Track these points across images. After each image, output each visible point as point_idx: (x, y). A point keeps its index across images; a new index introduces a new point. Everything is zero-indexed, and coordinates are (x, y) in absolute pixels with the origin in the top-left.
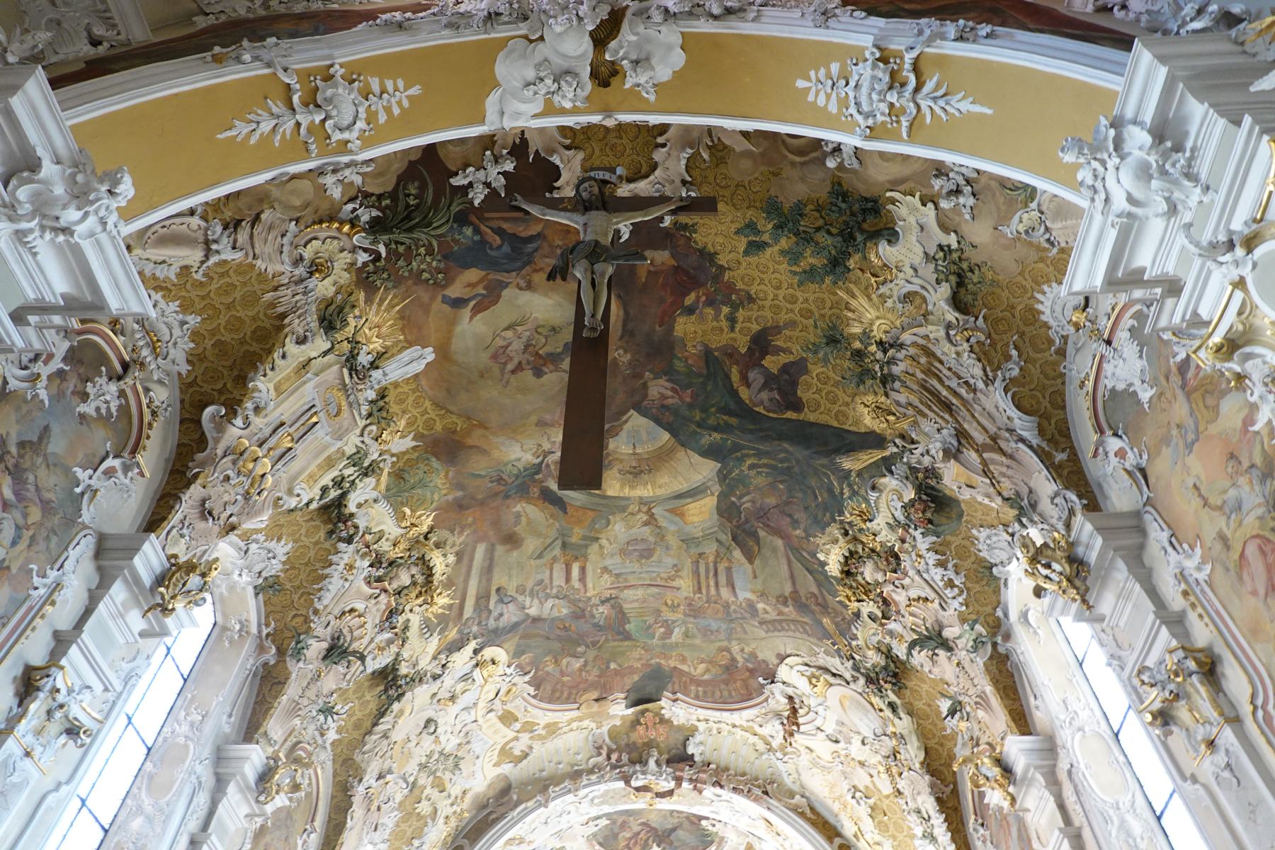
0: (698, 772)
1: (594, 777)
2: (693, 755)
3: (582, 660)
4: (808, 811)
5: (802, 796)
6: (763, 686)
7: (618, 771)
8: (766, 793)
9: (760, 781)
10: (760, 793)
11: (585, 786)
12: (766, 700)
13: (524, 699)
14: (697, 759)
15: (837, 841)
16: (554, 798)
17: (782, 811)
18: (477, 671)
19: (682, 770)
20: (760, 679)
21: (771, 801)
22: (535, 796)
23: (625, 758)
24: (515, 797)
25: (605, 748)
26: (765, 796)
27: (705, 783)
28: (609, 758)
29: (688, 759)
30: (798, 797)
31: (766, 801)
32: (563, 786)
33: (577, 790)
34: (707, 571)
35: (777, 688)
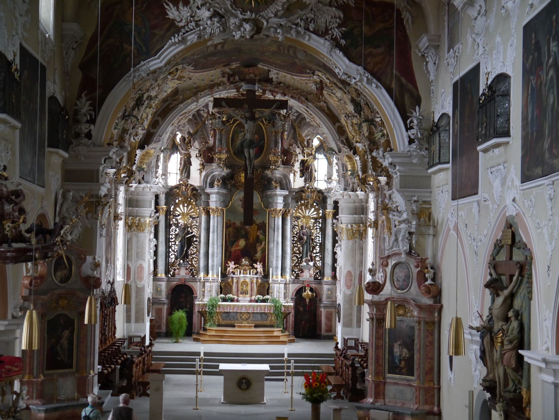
0: (275, 88)
1: (221, 88)
2: (272, 78)
3: (218, 57)
4: (326, 109)
5: (325, 102)
6: (309, 73)
7: (233, 85)
8: (307, 99)
9: (305, 93)
10: (304, 99)
11: (216, 92)
12: (310, 77)
13: (189, 72)
14: (274, 80)
15: (337, 124)
16: (201, 98)
17: (314, 109)
18: (169, 77)
19: (266, 87)
20: (308, 71)
21: (309, 103)
22: (191, 97)
23: (237, 78)
24: (181, 97)
25: (227, 76)
26: (306, 101)
27: (277, 93)
28: (229, 79)
29: (270, 81)
30: (322, 103)
31: (306, 103)
32: (205, 92)
33: (213, 94)
34: (284, 49)
35: (315, 77)
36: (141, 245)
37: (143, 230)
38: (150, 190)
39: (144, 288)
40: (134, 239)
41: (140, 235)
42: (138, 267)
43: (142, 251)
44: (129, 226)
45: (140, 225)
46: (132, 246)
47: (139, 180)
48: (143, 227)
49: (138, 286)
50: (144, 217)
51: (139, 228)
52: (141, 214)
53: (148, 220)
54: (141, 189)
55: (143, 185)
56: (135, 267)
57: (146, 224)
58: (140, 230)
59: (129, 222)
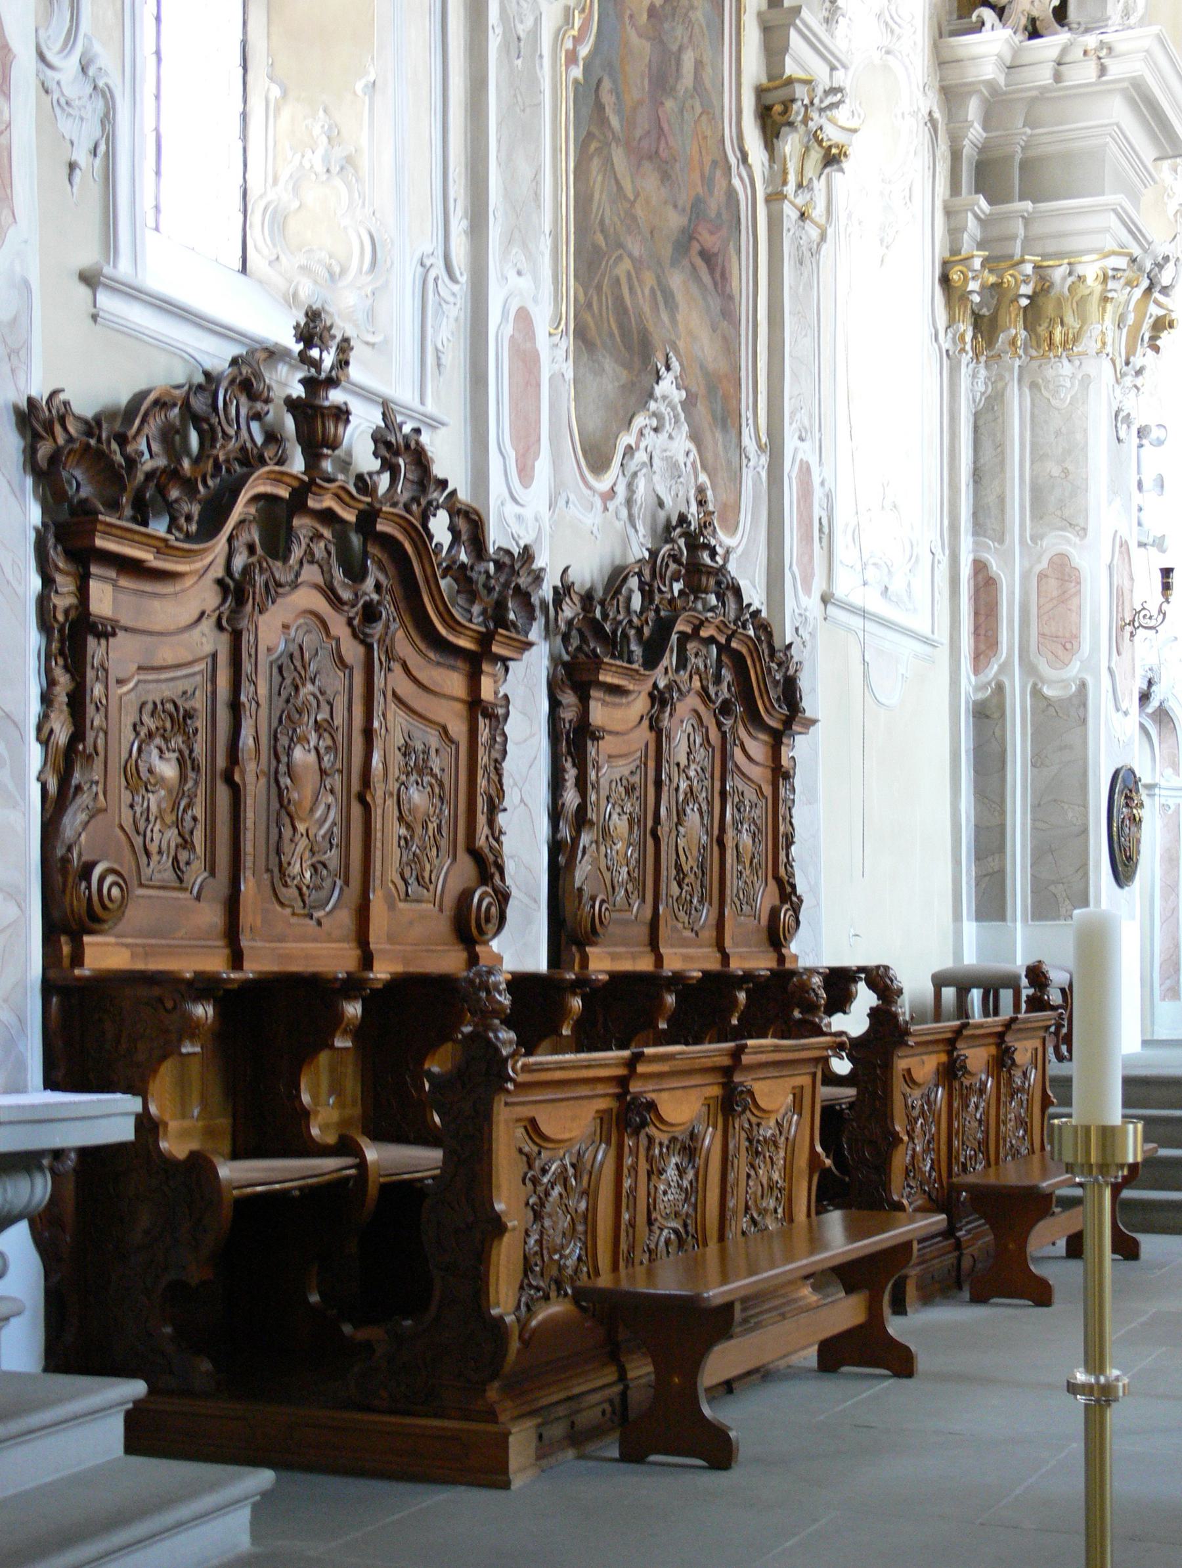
36: (1058, 433)
37: (1071, 341)
38: (1103, 70)
39: (1084, 705)
40: (1016, 402)
41: (1050, 373)
42: (1042, 576)
43: (1066, 472)
44: (978, 321)
45: (1050, 309)
46: (1000, 448)
47: (1033, 21)
48: (1070, 319)
49: (1047, 691)
50: (1071, 258)
51: (1042, 330)
52: (1051, 247)
53: (1090, 269)
54: (1045, 76)
55: (1054, 42)
56: (1025, 577)
57: (1083, 301)
58: (1051, 344)
59: (973, 286)
